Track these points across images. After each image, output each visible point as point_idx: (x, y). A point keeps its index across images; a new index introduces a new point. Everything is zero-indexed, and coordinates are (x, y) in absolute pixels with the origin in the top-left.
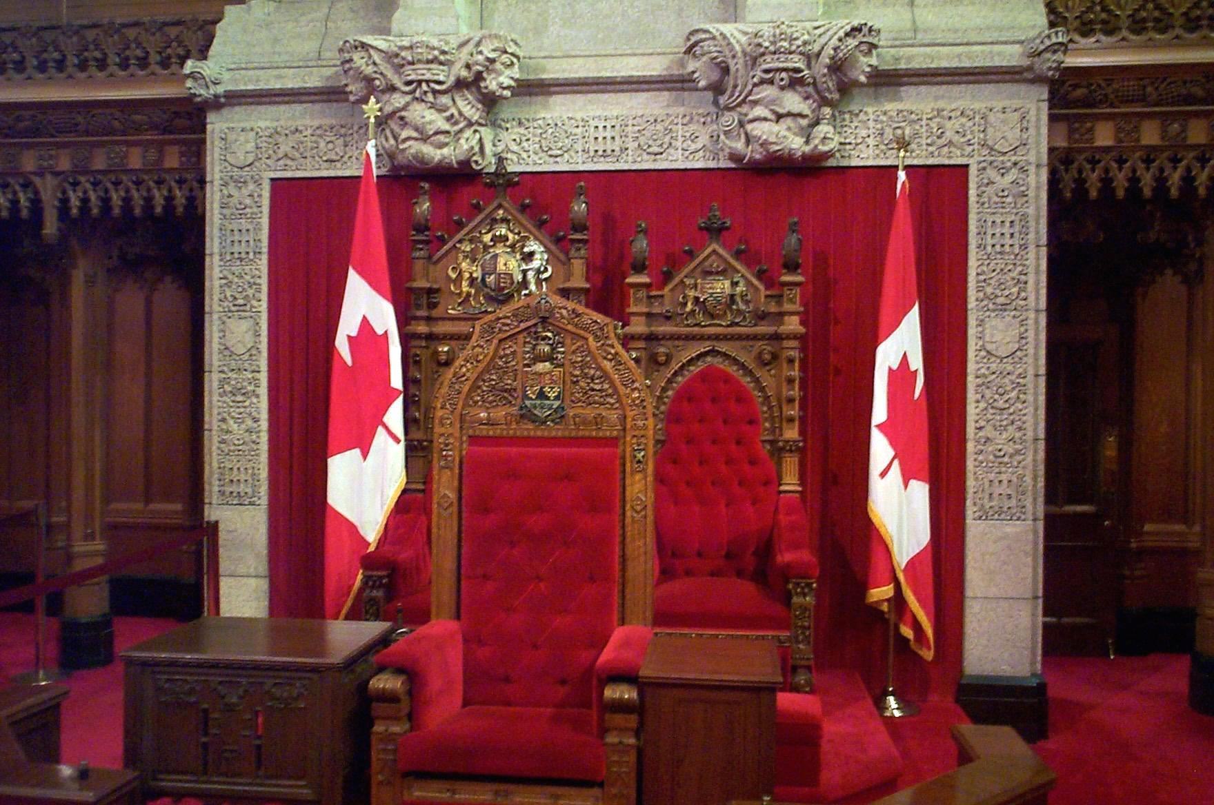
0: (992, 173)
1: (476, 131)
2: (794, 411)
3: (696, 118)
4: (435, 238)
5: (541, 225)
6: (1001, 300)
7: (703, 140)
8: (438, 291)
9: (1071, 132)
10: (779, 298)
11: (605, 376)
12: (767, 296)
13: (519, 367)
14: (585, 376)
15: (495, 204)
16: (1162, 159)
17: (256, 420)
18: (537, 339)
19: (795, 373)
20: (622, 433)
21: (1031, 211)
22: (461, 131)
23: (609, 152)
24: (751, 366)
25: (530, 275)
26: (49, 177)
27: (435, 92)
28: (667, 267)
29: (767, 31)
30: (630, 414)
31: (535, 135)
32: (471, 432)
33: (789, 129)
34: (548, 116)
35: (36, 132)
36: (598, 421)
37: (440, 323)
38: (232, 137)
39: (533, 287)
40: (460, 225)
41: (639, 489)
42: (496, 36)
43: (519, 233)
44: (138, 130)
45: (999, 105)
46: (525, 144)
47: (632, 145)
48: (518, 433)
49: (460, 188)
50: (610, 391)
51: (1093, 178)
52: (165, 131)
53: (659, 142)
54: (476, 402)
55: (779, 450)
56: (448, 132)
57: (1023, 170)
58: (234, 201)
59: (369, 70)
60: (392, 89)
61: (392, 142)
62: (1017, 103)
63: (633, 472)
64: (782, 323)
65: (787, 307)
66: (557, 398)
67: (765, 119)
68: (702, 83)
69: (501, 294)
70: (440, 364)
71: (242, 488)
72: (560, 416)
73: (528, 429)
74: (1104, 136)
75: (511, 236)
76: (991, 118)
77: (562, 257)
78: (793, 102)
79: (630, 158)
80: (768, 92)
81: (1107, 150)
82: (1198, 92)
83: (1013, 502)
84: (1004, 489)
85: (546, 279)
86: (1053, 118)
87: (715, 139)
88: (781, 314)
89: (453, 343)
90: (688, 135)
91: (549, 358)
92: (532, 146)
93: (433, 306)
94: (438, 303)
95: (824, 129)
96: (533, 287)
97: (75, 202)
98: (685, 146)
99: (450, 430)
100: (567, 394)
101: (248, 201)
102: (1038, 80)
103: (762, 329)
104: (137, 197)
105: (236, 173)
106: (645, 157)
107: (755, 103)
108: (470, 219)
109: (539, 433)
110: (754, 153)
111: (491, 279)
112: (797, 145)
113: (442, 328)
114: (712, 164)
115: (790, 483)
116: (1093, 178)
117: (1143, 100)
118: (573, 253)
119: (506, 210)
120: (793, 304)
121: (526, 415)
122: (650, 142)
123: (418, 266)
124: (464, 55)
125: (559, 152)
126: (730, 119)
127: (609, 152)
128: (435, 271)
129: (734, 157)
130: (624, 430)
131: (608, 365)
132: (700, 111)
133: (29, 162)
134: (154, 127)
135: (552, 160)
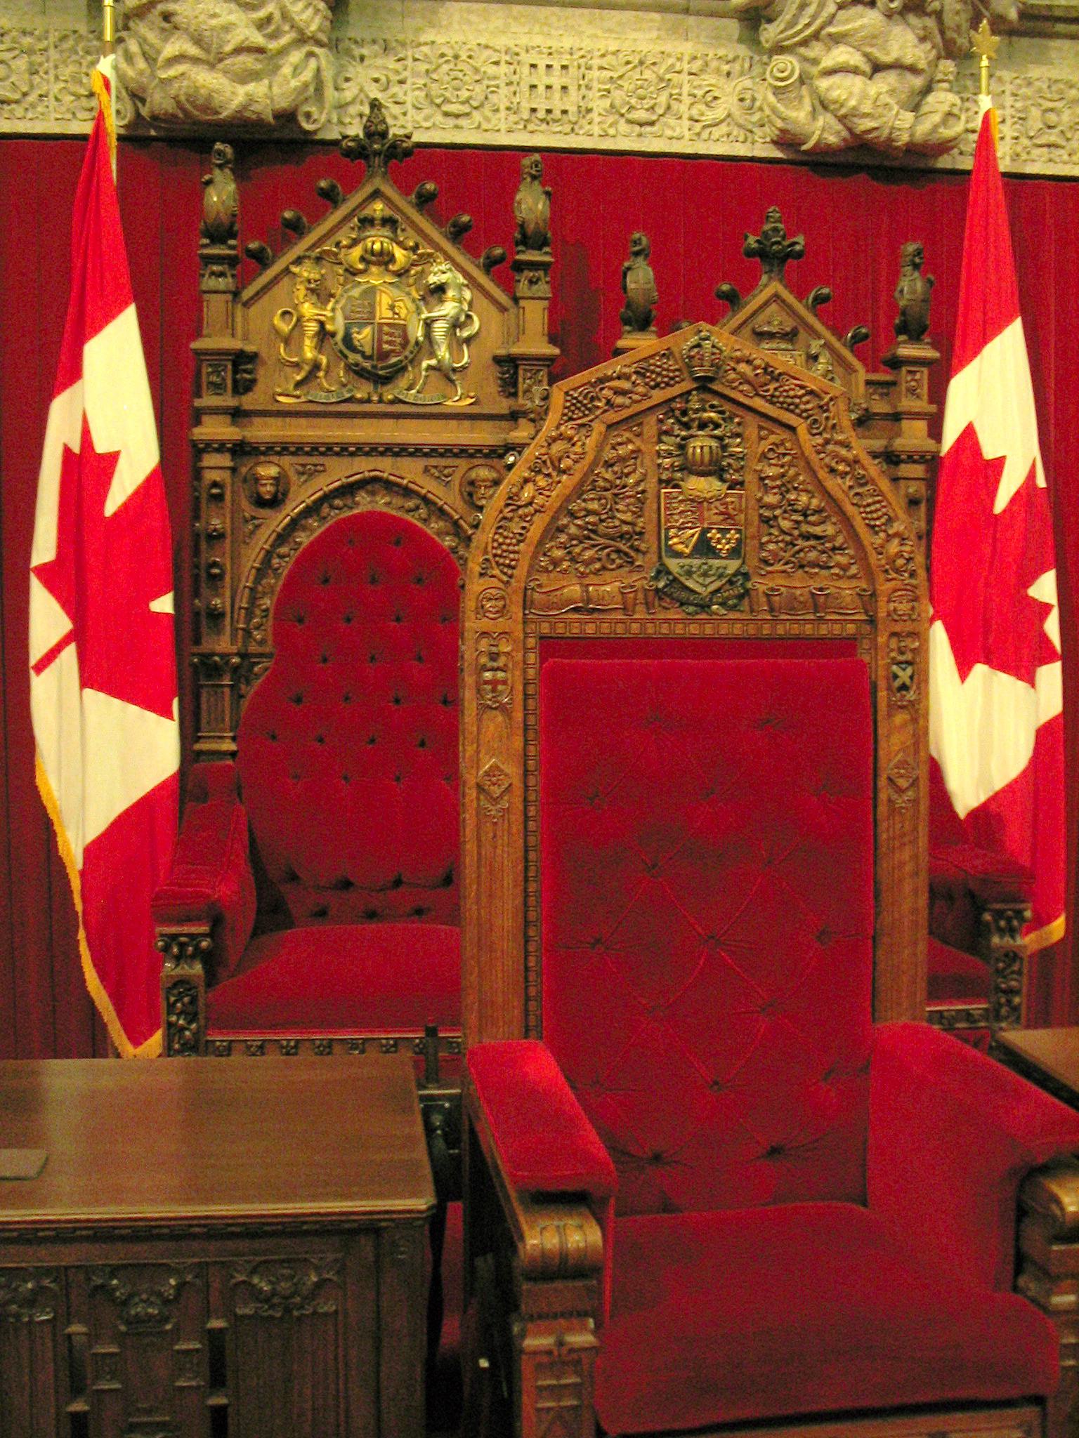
1: (311, 54)
3: (714, 64)
4: (253, 250)
5: (458, 234)
7: (727, 104)
8: (253, 357)
12: (868, 383)
13: (651, 485)
14: (792, 507)
15: (368, 189)
18: (687, 426)
20: (866, 628)
22: (283, 52)
23: (557, 114)
25: (440, 328)
30: (884, 587)
31: (416, 74)
32: (545, 629)
33: (892, 92)
34: (440, 39)
36: (817, 603)
37: (257, 421)
39: (443, 352)
40: (296, 229)
43: (414, 249)
46: (395, 89)
47: (600, 105)
48: (650, 629)
50: (839, 541)
53: (648, 103)
54: (556, 563)
56: (260, 50)
61: (141, 64)
63: (893, 708)
64: (899, 434)
65: (907, 404)
66: (735, 553)
67: (855, 71)
70: (261, 502)
72: (738, 590)
75: (399, 253)
77: (503, 298)
79: (596, 130)
85: (468, 341)
87: (748, 103)
88: (896, 417)
89: (287, 461)
90: (699, 93)
93: (243, 387)
94: (254, 381)
95: (941, 100)
96: (443, 352)
98: (694, 112)
99: (502, 624)
100: (751, 545)
106: (623, 127)
107: (837, 39)
108: (317, 218)
109: (693, 629)
110: (823, 131)
111: (364, 336)
113: (263, 431)
118: (522, 288)
119: (388, 202)
121: (671, 591)
122: (633, 101)
123: (215, 307)
125: (466, 109)
127: (557, 114)
129: (786, 140)
130: (872, 621)
132: (721, 52)
135: (451, 122)
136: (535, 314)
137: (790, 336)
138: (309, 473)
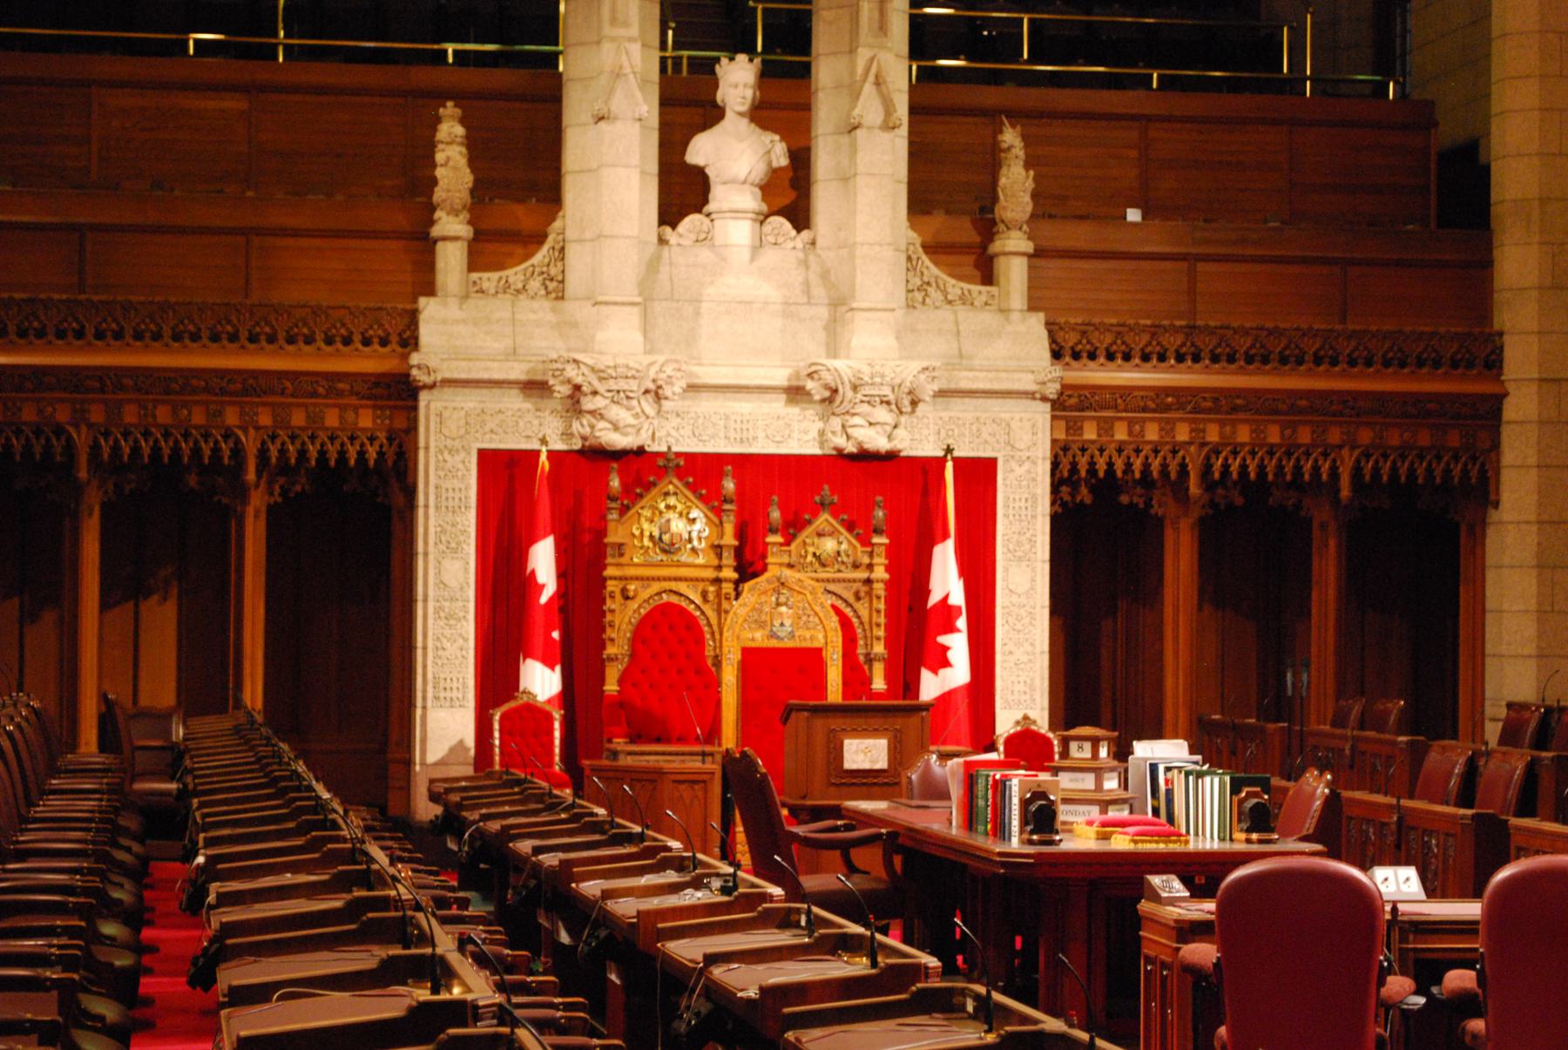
0: (1014, 465)
2: (881, 633)
6: (1019, 554)
7: (814, 434)
9: (1068, 429)
10: (871, 555)
11: (816, 614)
16: (1128, 451)
17: (466, 640)
19: (882, 606)
21: (1039, 491)
24: (851, 600)
26: (252, 432)
27: (628, 398)
28: (793, 527)
29: (866, 370)
30: (830, 634)
35: (246, 392)
38: (446, 414)
42: (676, 361)
44: (340, 394)
45: (1017, 416)
47: (761, 435)
51: (1083, 462)
52: (363, 398)
55: (870, 659)
57: (1034, 463)
58: (449, 465)
59: (579, 380)
60: (595, 393)
62: (1029, 415)
68: (817, 397)
69: (669, 548)
70: (627, 598)
71: (455, 694)
72: (792, 635)
73: (774, 643)
74: (1090, 433)
76: (1014, 425)
78: (883, 415)
80: (865, 408)
81: (1093, 442)
82: (1152, 405)
83: (1027, 697)
84: (1022, 687)
86: (1054, 418)
87: (822, 433)
91: (785, 604)
92: (687, 432)
97: (274, 453)
101: (460, 466)
102: (1044, 399)
103: (864, 575)
105: (449, 443)
110: (851, 448)
112: (878, 442)
114: (818, 452)
116: (1083, 462)
117: (1115, 407)
120: (880, 560)
121: (773, 635)
124: (652, 373)
126: (836, 423)
128: (621, 529)
131: (817, 609)
133: (231, 417)
134: (352, 393)
137: (831, 534)
138: (645, 587)
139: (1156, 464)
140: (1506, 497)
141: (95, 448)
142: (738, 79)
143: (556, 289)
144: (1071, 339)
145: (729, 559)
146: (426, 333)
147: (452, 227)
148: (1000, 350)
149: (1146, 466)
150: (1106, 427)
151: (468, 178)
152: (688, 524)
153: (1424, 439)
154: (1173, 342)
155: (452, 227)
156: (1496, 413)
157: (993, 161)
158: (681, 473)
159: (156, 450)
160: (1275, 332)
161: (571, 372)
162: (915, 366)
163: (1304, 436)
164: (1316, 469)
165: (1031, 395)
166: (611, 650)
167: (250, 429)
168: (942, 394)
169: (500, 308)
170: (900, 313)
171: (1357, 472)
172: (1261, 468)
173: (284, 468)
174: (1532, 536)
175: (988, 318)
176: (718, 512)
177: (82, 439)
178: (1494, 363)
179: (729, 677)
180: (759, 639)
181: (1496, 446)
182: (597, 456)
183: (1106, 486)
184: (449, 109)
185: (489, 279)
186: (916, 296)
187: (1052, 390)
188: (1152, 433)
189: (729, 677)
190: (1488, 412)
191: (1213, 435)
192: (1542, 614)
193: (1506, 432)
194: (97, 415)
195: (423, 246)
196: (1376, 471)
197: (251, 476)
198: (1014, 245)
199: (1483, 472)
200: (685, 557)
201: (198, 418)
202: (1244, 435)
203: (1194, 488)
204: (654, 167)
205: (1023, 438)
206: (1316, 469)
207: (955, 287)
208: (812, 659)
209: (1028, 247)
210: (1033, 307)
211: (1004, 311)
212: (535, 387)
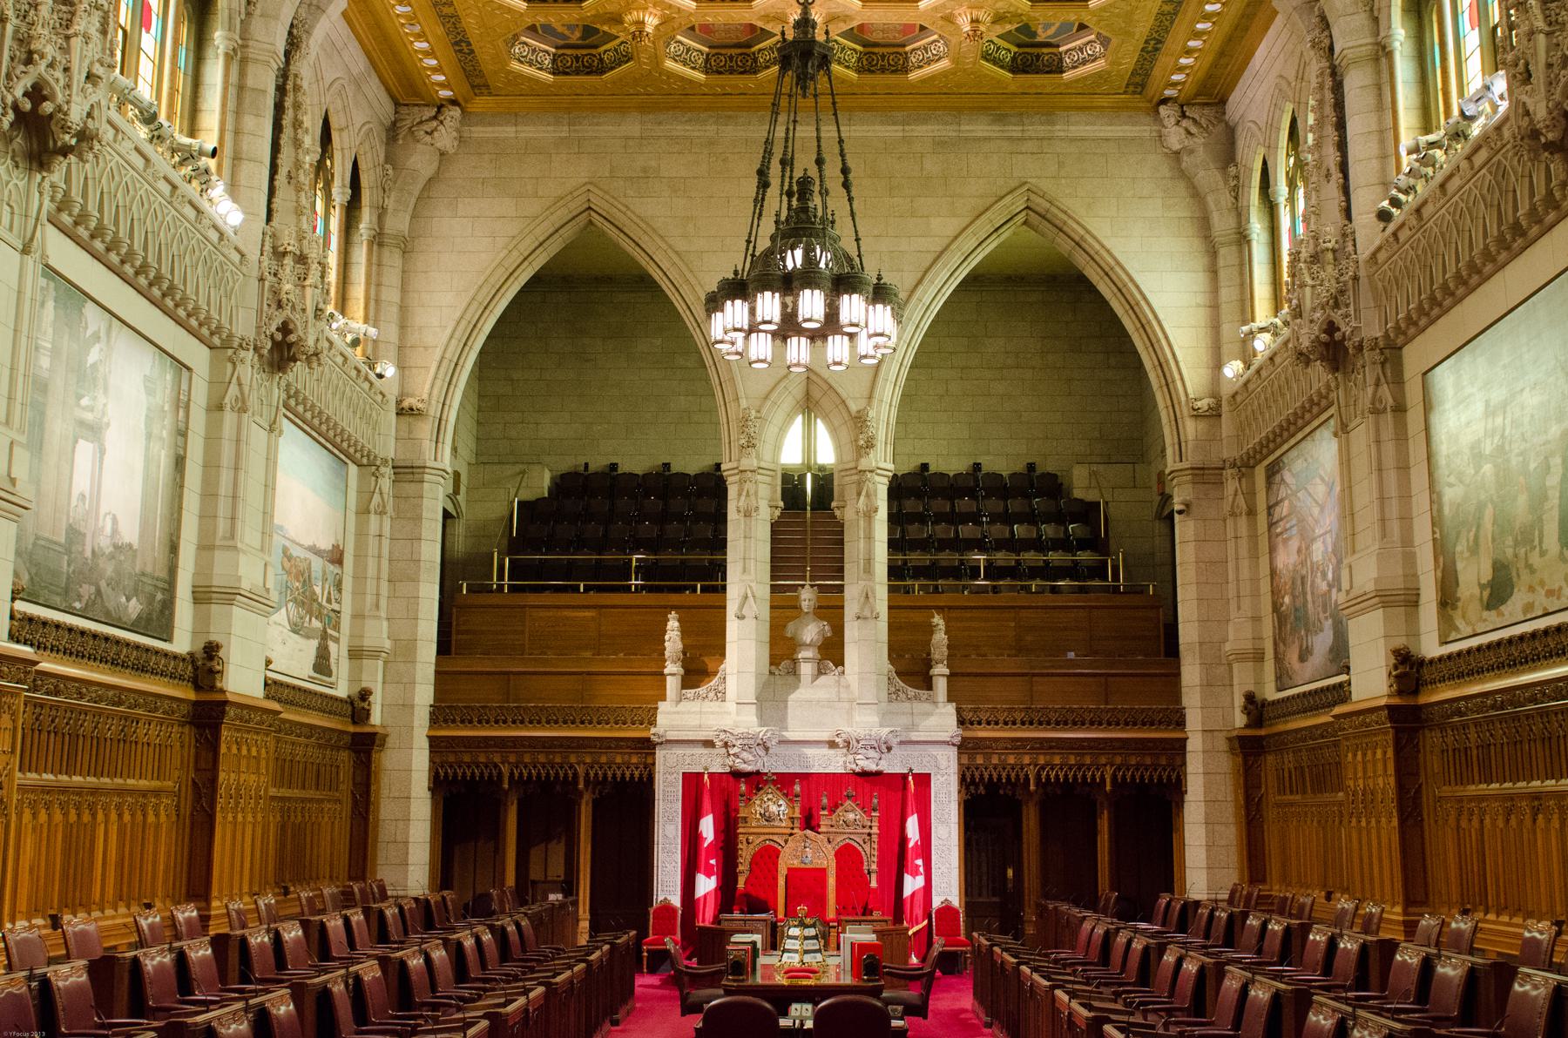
41: (832, 881)
49: (756, 780)
51: (977, 774)
74: (980, 760)
78: (872, 753)
104: (619, 773)
110: (858, 770)
112: (873, 767)
115: (874, 884)
116: (977, 774)
126: (851, 757)
133: (573, 759)
136: (797, 810)
139: (1013, 775)
140: (1189, 789)
141: (512, 774)
142: (807, 597)
143: (720, 695)
144: (968, 716)
145: (797, 824)
146: (660, 719)
147: (673, 668)
148: (932, 721)
149: (1008, 776)
150: (988, 757)
151: (680, 646)
152: (777, 806)
153: (1148, 761)
154: (1019, 716)
155: (673, 668)
156: (1184, 747)
157: (930, 630)
158: (775, 783)
159: (539, 774)
160: (1072, 711)
161: (722, 736)
162: (886, 730)
163: (1088, 761)
164: (1093, 776)
165: (947, 743)
166: (741, 868)
167: (581, 765)
168: (901, 743)
169: (695, 706)
170: (884, 705)
171: (1114, 777)
172: (1066, 776)
173: (597, 783)
174: (1202, 808)
175: (927, 707)
176: (791, 801)
177: (505, 770)
178: (1181, 723)
179: (781, 882)
180: (796, 863)
181: (1184, 764)
182: (736, 775)
183: (992, 786)
184: (673, 615)
185: (690, 693)
186: (894, 696)
187: (957, 740)
188: (1011, 760)
189: (781, 882)
190: (1178, 748)
191: (1042, 761)
192: (1209, 847)
193: (1189, 757)
194: (512, 758)
195: (661, 676)
196: (1124, 776)
197: (581, 786)
198: (940, 670)
199: (1178, 776)
200: (776, 823)
201: (558, 760)
202: (1057, 760)
203: (1032, 788)
204: (766, 637)
205: (943, 763)
206: (1093, 776)
207: (911, 692)
208: (821, 873)
209: (947, 671)
210: (949, 700)
211: (935, 703)
212: (709, 744)
